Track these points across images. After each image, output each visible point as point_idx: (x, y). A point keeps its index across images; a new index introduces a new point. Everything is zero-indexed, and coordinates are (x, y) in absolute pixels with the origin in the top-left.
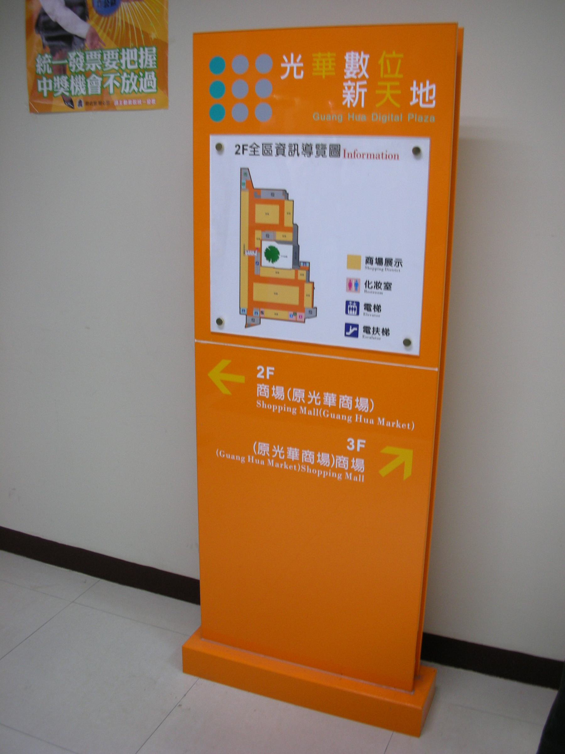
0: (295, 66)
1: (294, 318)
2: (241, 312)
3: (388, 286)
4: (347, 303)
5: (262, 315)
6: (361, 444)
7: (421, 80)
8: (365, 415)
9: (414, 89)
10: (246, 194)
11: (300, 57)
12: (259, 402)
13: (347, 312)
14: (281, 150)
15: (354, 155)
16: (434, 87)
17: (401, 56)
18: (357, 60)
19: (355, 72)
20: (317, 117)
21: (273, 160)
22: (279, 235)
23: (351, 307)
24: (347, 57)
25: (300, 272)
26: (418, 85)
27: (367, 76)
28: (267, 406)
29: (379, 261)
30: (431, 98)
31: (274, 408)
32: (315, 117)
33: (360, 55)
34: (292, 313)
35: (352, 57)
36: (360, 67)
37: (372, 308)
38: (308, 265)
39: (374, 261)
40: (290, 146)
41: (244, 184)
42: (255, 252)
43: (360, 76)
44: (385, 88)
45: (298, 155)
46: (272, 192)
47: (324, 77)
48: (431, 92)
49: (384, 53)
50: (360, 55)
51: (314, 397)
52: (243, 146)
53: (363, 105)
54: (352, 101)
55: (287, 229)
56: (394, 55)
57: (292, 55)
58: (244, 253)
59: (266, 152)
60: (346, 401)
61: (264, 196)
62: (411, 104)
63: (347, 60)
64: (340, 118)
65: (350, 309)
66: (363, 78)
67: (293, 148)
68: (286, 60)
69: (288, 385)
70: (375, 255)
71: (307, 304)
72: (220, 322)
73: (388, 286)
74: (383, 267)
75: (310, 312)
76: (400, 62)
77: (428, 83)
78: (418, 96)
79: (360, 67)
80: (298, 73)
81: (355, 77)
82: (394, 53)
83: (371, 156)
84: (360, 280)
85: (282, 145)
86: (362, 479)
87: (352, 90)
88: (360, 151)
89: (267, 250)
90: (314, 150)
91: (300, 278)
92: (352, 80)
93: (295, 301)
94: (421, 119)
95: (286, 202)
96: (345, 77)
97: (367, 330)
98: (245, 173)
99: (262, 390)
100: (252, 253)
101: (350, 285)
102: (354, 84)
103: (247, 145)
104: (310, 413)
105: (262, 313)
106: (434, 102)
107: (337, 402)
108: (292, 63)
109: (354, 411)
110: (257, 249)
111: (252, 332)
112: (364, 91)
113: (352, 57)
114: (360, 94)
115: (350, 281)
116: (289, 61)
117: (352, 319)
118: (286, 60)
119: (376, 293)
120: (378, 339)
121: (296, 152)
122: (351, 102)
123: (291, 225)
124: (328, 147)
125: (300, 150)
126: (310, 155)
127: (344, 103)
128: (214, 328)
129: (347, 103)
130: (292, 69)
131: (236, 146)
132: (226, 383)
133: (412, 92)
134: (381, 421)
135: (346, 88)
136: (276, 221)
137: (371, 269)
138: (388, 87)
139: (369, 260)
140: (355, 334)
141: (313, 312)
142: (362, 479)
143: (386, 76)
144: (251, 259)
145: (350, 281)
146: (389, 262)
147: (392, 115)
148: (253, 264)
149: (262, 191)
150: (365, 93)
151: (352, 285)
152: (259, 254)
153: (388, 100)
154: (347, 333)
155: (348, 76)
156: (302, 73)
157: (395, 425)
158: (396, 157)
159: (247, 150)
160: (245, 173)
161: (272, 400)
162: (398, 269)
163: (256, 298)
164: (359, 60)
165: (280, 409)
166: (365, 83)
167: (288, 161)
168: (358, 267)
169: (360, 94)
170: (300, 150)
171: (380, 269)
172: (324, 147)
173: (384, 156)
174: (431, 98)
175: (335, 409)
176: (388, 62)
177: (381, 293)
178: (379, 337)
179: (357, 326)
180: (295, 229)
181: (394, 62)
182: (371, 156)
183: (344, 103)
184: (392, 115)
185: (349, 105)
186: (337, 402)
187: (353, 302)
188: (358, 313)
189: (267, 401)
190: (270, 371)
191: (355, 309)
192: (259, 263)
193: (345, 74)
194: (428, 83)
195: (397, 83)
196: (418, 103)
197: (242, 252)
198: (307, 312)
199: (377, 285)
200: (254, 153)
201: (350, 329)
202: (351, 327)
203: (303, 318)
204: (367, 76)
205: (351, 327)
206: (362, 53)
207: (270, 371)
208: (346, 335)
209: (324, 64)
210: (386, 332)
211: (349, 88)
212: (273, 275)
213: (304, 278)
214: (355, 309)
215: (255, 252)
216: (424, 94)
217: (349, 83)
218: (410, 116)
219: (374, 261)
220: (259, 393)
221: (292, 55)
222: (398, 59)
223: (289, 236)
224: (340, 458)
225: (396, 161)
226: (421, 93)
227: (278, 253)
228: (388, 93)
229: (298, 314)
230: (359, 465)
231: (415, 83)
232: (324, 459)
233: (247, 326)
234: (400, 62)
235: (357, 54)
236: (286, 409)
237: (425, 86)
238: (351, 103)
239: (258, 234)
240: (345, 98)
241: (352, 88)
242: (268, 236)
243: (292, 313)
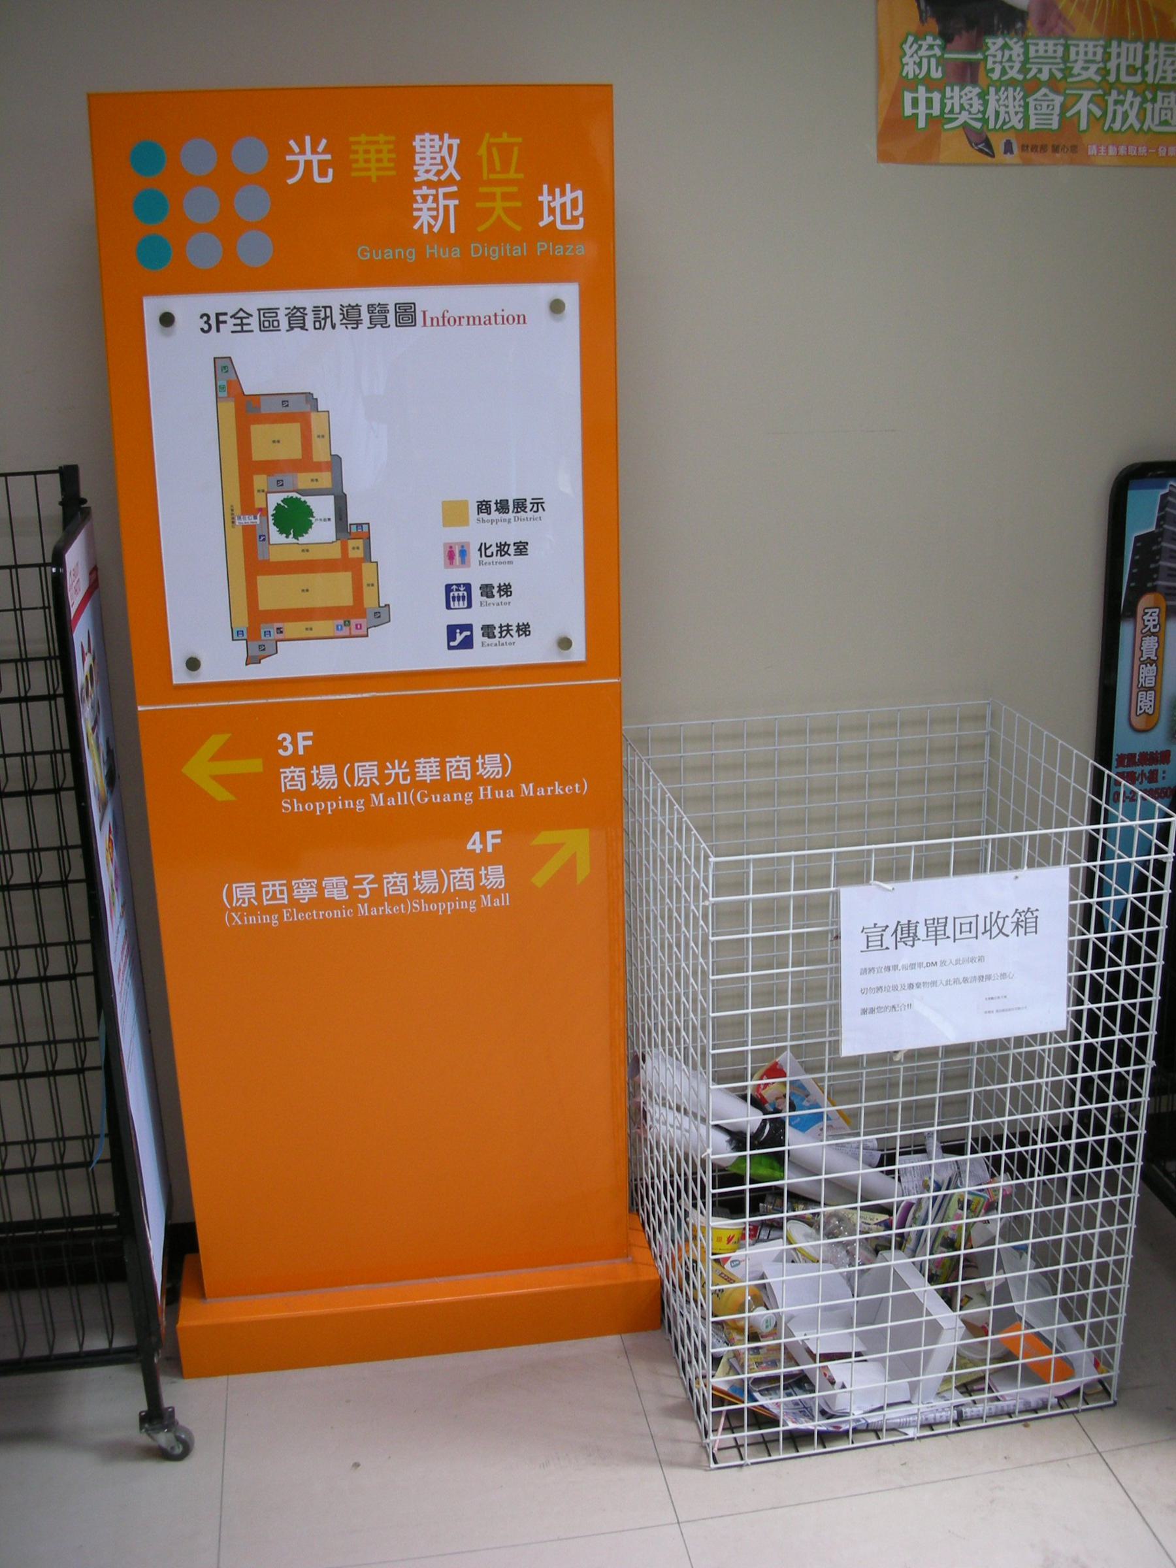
0: (315, 159)
1: (346, 631)
2: (236, 635)
3: (522, 548)
4: (448, 588)
5: (280, 636)
6: (493, 838)
7: (556, 183)
8: (497, 784)
9: (545, 198)
10: (229, 407)
11: (324, 142)
12: (286, 802)
13: (448, 607)
14: (297, 318)
15: (444, 320)
16: (579, 194)
17: (520, 140)
18: (437, 149)
19: (435, 169)
20: (364, 253)
21: (286, 339)
22: (304, 480)
23: (456, 594)
24: (417, 143)
25: (352, 543)
26: (551, 193)
27: (458, 178)
28: (304, 808)
29: (503, 506)
30: (576, 213)
31: (319, 807)
32: (363, 251)
33: (442, 139)
34: (341, 622)
35: (428, 143)
36: (443, 158)
37: (495, 591)
38: (365, 528)
39: (493, 507)
40: (316, 310)
41: (223, 388)
42: (255, 518)
43: (443, 178)
44: (491, 197)
45: (333, 327)
46: (284, 399)
47: (374, 180)
48: (574, 202)
49: (487, 135)
50: (442, 139)
51: (396, 770)
52: (218, 315)
53: (452, 230)
54: (433, 223)
55: (319, 467)
56: (505, 138)
57: (308, 139)
58: (233, 522)
59: (266, 324)
60: (459, 766)
61: (265, 409)
62: (542, 224)
63: (418, 149)
64: (411, 253)
65: (454, 600)
66: (450, 181)
67: (322, 315)
68: (296, 149)
69: (342, 759)
70: (493, 497)
71: (369, 602)
72: (193, 664)
73: (522, 548)
74: (511, 515)
75: (377, 615)
76: (516, 149)
77: (568, 186)
78: (552, 211)
79: (443, 158)
80: (323, 174)
81: (435, 179)
82: (505, 134)
83: (473, 320)
84: (468, 544)
85: (298, 309)
86: (506, 900)
87: (430, 204)
88: (454, 313)
89: (278, 507)
90: (365, 316)
91: (352, 554)
92: (429, 184)
93: (347, 600)
94: (559, 250)
95: (314, 415)
96: (417, 179)
97: (488, 631)
98: (223, 366)
99: (292, 778)
100: (249, 520)
101: (451, 556)
102: (433, 192)
103: (225, 314)
104: (391, 802)
105: (280, 631)
106: (581, 220)
107: (443, 772)
108: (309, 156)
109: (478, 780)
110: (260, 510)
111: (268, 670)
112: (452, 203)
113: (428, 143)
114: (446, 208)
115: (451, 547)
116: (303, 152)
117: (459, 616)
118: (297, 150)
119: (500, 563)
120: (510, 644)
121: (329, 320)
122: (429, 224)
123: (327, 458)
124: (391, 308)
125: (337, 317)
126: (357, 328)
127: (416, 227)
128: (180, 676)
129: (422, 226)
130: (308, 164)
131: (202, 317)
132: (222, 780)
133: (542, 202)
134: (528, 790)
135: (419, 199)
136: (297, 454)
137: (488, 521)
138: (498, 196)
139: (483, 507)
140: (467, 643)
141: (382, 615)
142: (506, 900)
143: (492, 176)
144: (248, 530)
145: (451, 547)
146: (520, 505)
147: (508, 247)
148: (253, 539)
149: (262, 398)
150: (455, 206)
151: (455, 555)
152: (265, 518)
153: (499, 218)
154: (452, 644)
155: (421, 177)
156: (330, 171)
157: (553, 791)
158: (520, 319)
159: (225, 322)
160: (223, 366)
161: (314, 794)
162: (536, 515)
163: (265, 604)
164: (441, 148)
165: (331, 806)
166: (454, 189)
167: (308, 338)
168: (464, 522)
169: (446, 208)
170: (337, 317)
171: (505, 520)
172: (383, 308)
173: (499, 319)
174: (575, 213)
175: (439, 786)
176: (495, 151)
177: (510, 563)
178: (512, 640)
179: (469, 627)
180: (335, 464)
181: (505, 150)
182: (473, 320)
183: (416, 227)
184: (508, 247)
185: (426, 231)
186: (443, 772)
187: (458, 585)
188: (470, 606)
189: (303, 797)
190: (304, 739)
191: (463, 600)
192: (265, 538)
193: (415, 174)
194: (568, 186)
195: (514, 189)
196: (554, 222)
197: (229, 519)
198: (370, 615)
199: (502, 549)
200: (242, 328)
201: (458, 635)
202: (458, 631)
203: (364, 629)
204: (458, 178)
205: (458, 631)
206: (446, 136)
207: (305, 739)
208: (450, 648)
209: (373, 156)
210: (524, 629)
211: (425, 198)
212: (297, 555)
213: (359, 554)
214: (463, 600)
215: (255, 518)
216: (563, 206)
217: (425, 190)
218: (541, 247)
219: (493, 507)
220: (285, 785)
221: (308, 139)
222: (513, 145)
223: (325, 480)
224: (457, 873)
225: (522, 326)
226: (557, 204)
227: (311, 514)
228: (499, 206)
229: (353, 622)
230: (495, 876)
231: (545, 187)
232: (427, 880)
233: (251, 660)
234: (516, 149)
235: (436, 137)
236: (344, 804)
237: (563, 194)
238: (430, 227)
239: (260, 481)
240: (419, 217)
241: (431, 198)
242: (280, 483)
243: (341, 622)
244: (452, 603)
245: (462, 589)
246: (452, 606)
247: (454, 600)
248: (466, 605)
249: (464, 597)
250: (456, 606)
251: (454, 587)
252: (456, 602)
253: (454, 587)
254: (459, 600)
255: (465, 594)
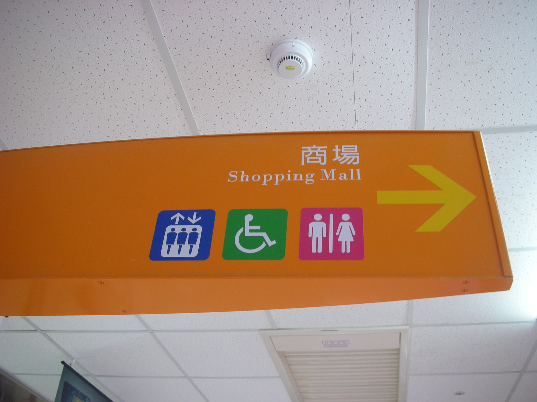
187: (188, 213)
191: (193, 240)
244: (165, 247)
245: (194, 221)
246: (164, 253)
247: (170, 241)
248: (195, 253)
249: (193, 237)
250: (174, 253)
251: (178, 216)
252: (175, 247)
253: (178, 216)
254: (181, 241)
255: (199, 229)
